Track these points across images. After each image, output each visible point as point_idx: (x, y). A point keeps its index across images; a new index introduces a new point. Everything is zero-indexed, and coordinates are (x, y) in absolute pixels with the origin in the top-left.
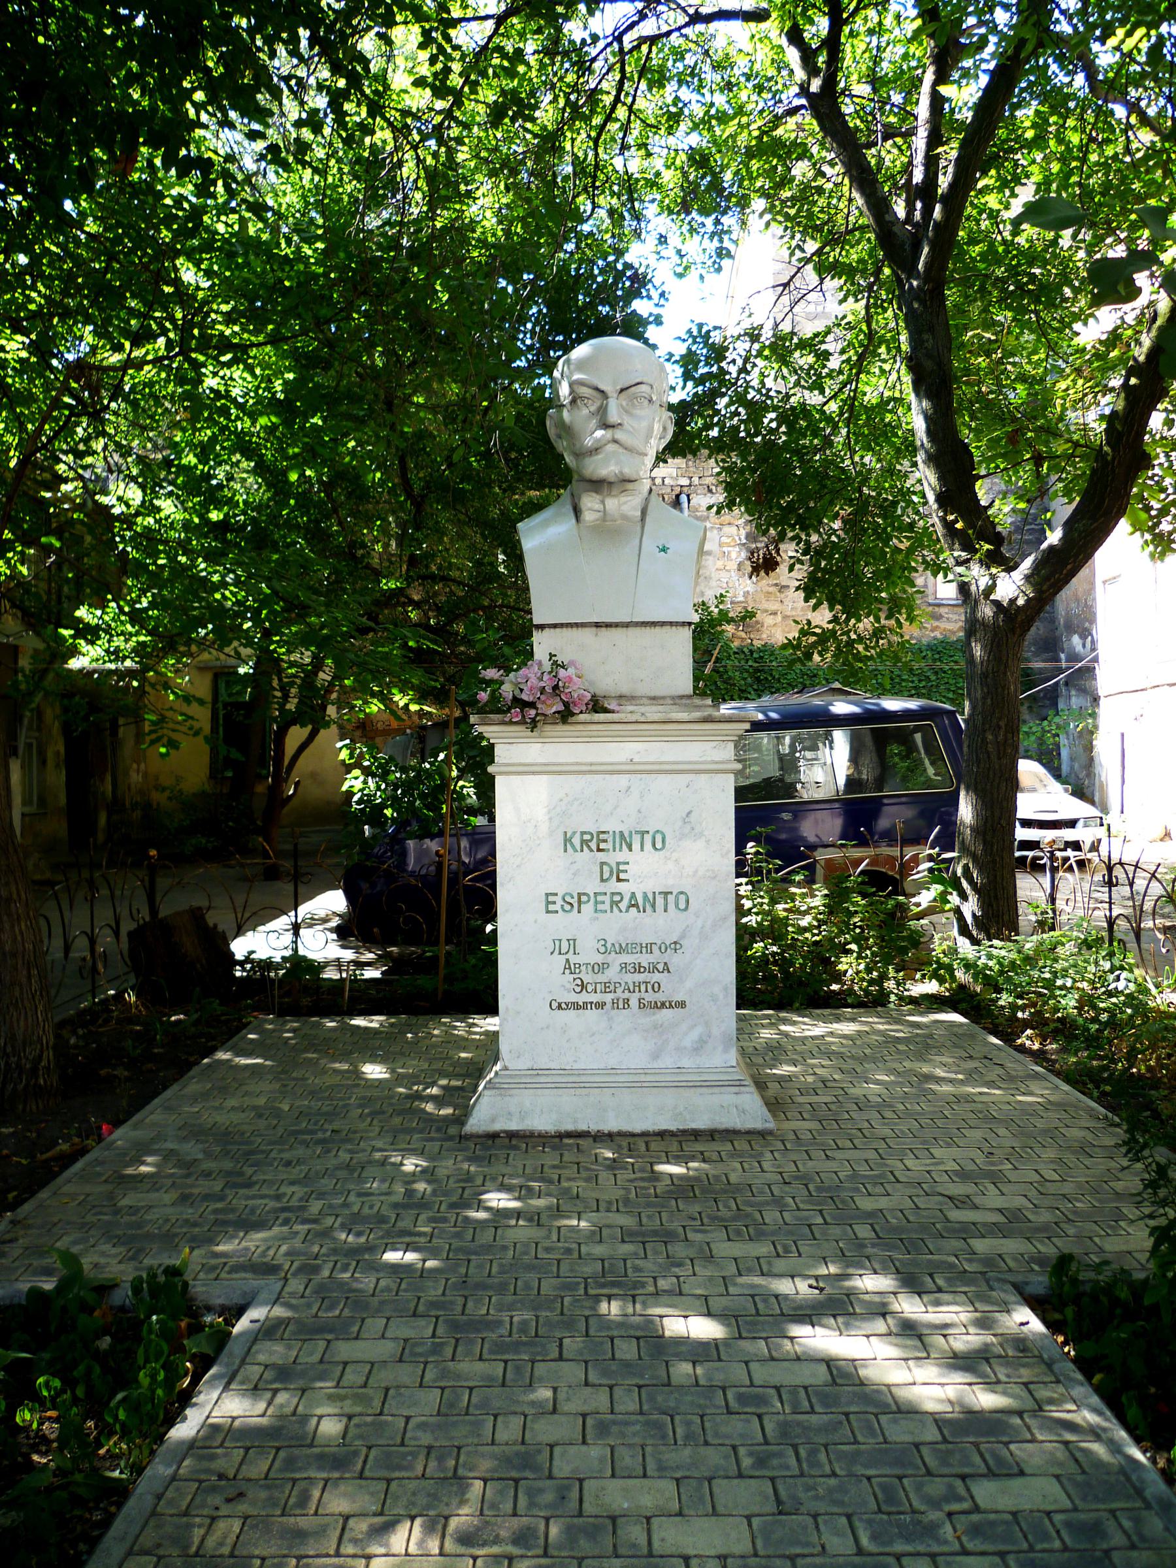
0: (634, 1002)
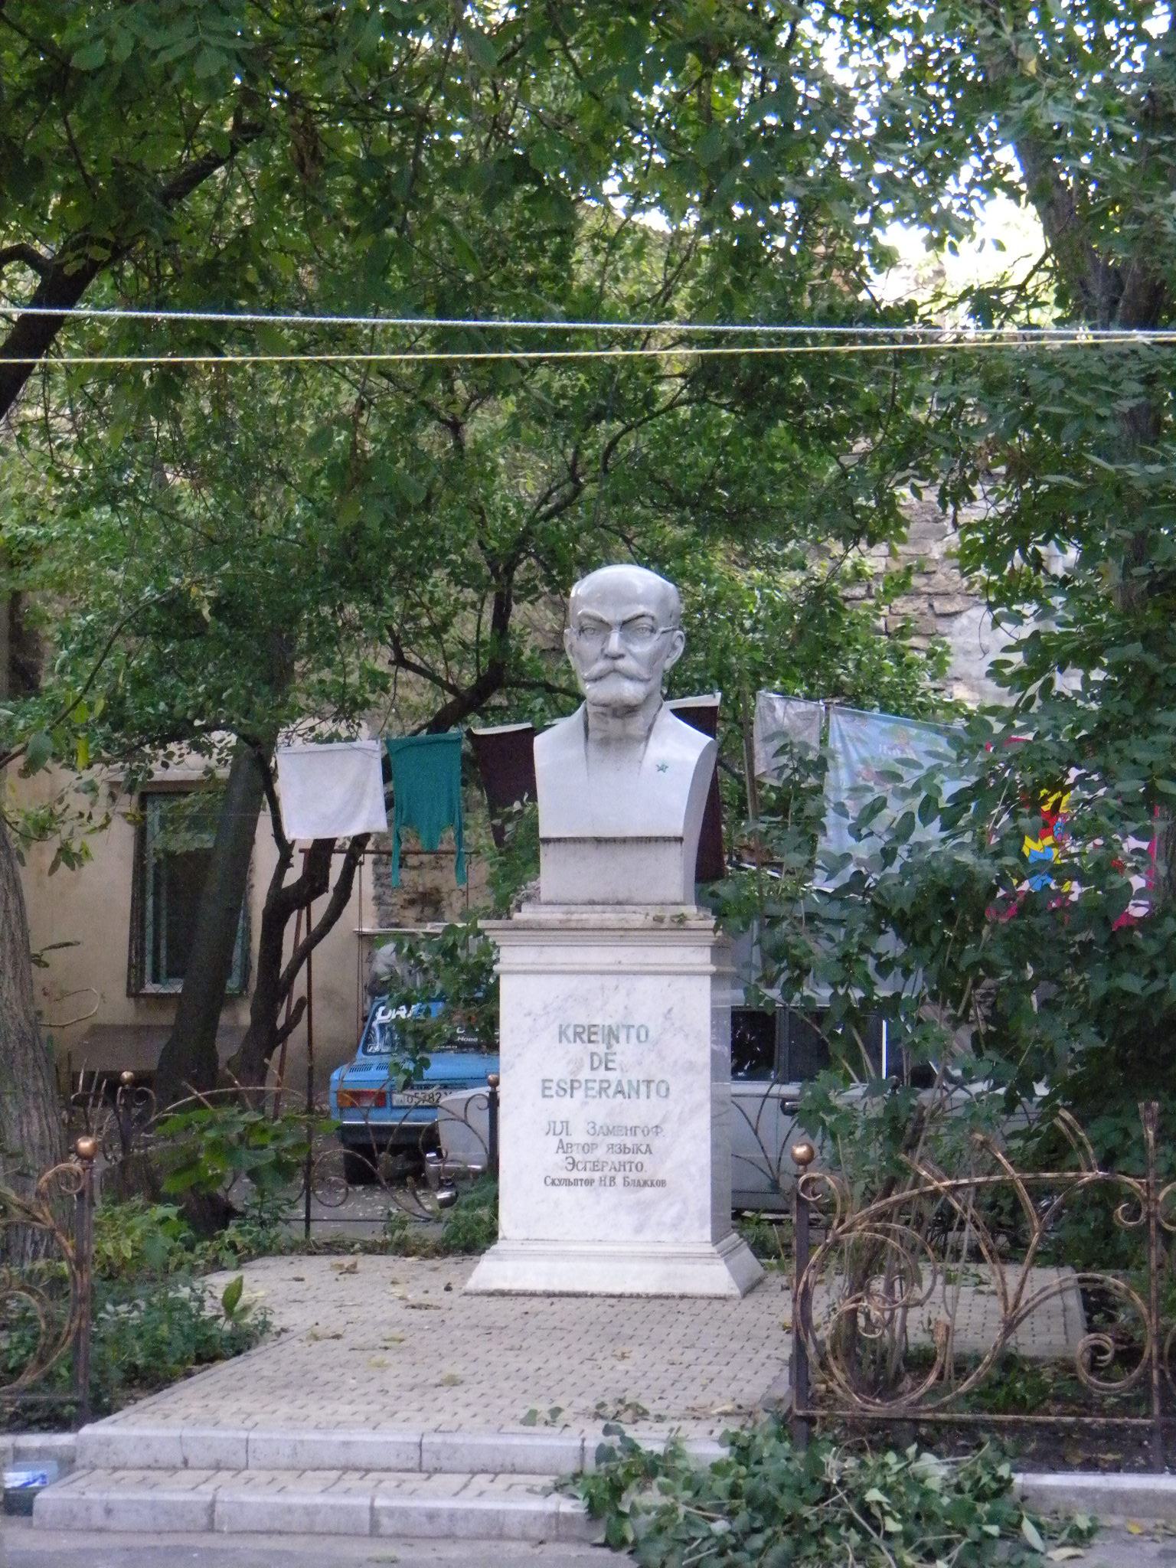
0: (619, 1180)
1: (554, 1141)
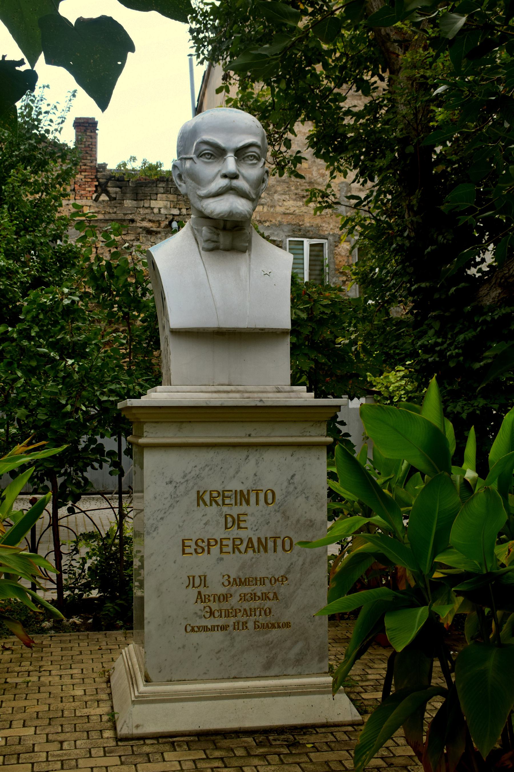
0: (250, 625)
1: (193, 593)
